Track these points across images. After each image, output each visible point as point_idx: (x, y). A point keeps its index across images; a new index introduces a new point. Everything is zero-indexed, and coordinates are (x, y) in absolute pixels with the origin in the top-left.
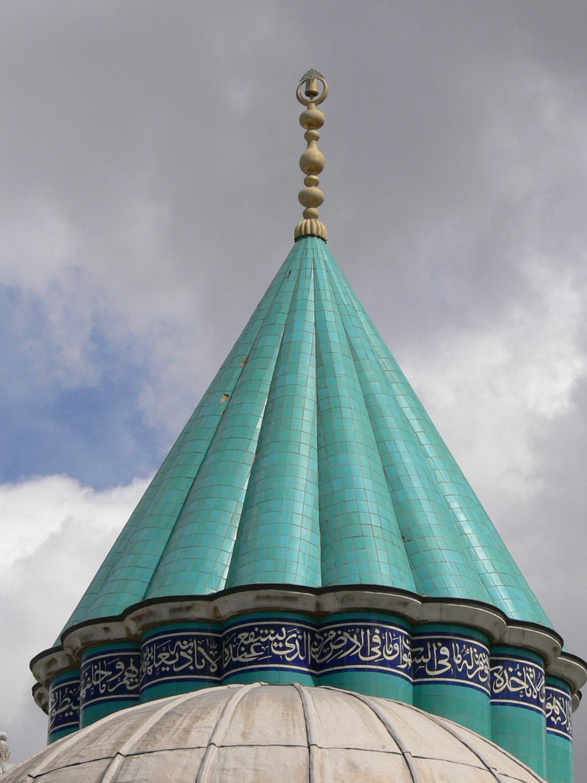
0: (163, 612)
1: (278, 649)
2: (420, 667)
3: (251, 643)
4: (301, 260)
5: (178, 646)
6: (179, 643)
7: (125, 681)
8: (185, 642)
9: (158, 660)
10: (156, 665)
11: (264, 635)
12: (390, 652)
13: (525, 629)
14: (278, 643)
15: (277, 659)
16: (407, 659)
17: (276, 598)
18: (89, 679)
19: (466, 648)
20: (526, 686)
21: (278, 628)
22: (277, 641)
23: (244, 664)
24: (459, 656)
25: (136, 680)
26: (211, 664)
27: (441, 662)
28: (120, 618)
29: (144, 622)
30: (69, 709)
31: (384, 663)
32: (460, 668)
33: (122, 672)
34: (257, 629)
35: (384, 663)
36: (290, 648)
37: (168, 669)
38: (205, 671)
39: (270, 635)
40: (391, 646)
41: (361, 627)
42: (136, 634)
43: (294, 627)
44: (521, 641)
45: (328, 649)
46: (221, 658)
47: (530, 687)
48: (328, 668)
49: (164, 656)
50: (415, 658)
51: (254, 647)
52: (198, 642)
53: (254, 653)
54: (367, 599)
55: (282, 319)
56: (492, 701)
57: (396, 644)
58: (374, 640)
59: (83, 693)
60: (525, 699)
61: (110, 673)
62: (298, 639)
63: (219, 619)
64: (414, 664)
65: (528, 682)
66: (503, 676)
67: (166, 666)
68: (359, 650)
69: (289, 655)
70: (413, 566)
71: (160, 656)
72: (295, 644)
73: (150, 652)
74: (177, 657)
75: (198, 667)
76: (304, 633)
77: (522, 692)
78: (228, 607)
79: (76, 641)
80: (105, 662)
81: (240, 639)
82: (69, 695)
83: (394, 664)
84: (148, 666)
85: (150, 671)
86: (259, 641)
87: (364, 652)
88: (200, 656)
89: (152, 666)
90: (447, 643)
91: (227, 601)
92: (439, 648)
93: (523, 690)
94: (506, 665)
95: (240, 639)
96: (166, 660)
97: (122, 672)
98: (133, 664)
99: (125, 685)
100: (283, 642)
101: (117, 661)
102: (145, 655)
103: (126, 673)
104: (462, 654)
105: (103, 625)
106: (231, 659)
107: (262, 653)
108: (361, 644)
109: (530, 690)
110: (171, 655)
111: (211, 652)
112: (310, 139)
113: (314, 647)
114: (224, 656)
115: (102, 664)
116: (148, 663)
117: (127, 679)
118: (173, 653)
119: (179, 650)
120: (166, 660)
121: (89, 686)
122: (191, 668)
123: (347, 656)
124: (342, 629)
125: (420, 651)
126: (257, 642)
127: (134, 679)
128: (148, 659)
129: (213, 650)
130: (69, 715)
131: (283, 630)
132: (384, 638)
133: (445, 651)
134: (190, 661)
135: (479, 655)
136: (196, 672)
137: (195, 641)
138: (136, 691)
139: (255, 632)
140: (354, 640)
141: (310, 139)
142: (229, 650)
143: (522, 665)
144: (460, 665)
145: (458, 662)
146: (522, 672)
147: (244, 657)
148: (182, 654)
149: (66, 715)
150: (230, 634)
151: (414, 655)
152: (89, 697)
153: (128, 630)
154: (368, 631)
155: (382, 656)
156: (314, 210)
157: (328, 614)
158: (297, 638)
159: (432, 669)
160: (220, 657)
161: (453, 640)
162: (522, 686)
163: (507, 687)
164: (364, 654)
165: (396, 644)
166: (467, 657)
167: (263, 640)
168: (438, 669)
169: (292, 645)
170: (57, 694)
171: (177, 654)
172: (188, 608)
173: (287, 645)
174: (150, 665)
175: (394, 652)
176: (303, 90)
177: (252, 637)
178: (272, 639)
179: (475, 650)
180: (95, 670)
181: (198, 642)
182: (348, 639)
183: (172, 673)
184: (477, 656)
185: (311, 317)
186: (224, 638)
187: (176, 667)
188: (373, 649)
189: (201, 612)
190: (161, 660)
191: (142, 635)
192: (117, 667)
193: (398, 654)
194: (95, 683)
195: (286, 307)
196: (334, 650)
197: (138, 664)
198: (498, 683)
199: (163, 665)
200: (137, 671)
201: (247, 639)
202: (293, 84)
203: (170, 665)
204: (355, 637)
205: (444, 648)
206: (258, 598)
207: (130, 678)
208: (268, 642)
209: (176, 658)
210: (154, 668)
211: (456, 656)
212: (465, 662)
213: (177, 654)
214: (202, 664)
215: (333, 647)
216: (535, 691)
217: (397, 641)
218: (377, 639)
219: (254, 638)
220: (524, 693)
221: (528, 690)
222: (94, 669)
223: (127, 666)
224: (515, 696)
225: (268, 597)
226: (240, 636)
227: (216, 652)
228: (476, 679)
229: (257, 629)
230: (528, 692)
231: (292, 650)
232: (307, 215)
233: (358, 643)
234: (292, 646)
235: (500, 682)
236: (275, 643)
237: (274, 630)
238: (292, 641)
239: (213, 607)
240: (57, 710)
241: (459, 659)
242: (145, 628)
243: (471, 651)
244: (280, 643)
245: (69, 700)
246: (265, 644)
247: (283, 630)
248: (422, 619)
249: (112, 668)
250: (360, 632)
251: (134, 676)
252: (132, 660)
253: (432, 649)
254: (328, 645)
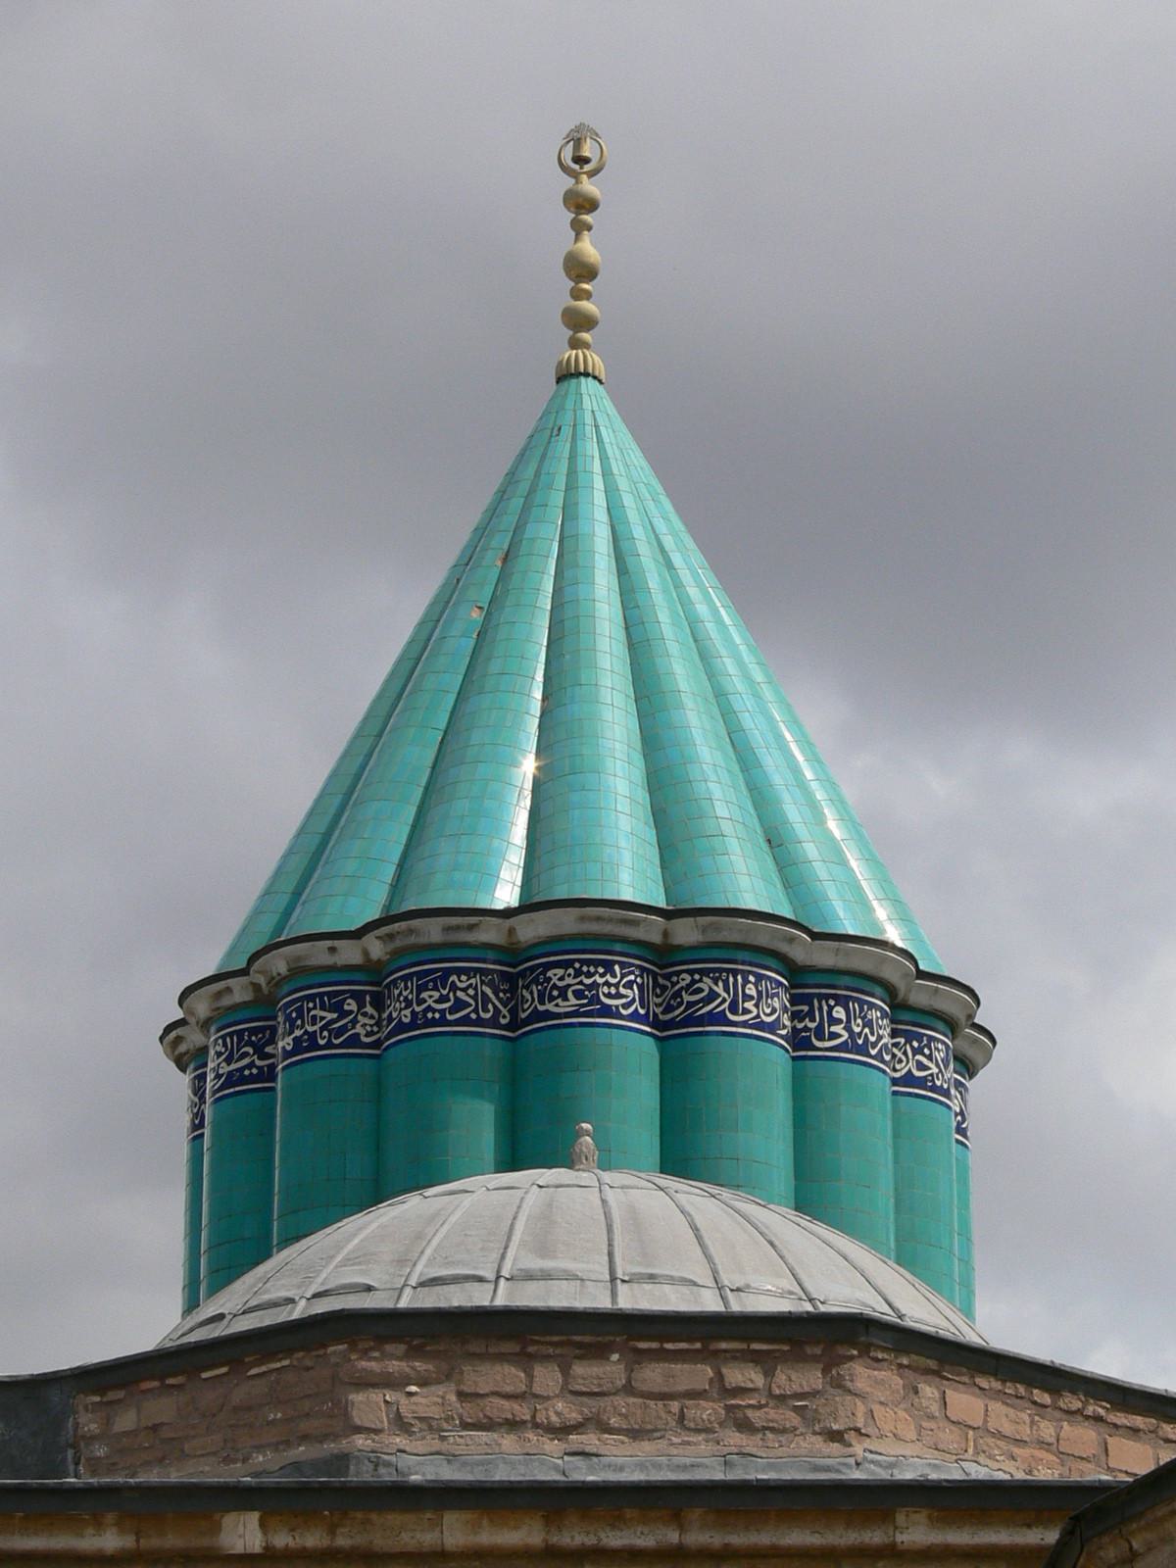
0: (433, 931)
1: (609, 996)
2: (803, 1034)
3: (569, 986)
4: (575, 411)
5: (453, 982)
6: (454, 978)
7: (358, 1029)
8: (463, 978)
9: (420, 1002)
10: (418, 1009)
11: (589, 975)
12: (768, 1011)
13: (940, 986)
14: (609, 988)
15: (607, 1011)
16: (786, 1020)
17: (610, 920)
18: (299, 1022)
19: (868, 1010)
20: (936, 1070)
21: (608, 967)
22: (607, 983)
23: (558, 1016)
24: (859, 1021)
25: (375, 1029)
26: (500, 1011)
27: (834, 1029)
28: (357, 934)
29: (398, 943)
30: (251, 1065)
31: (761, 1026)
32: (860, 1038)
33: (353, 1015)
34: (577, 965)
35: (761, 1026)
36: (623, 996)
37: (437, 1015)
38: (494, 1022)
39: (597, 975)
40: (769, 1001)
41: (728, 971)
42: (379, 960)
43: (633, 965)
44: (932, 1003)
45: (679, 1000)
46: (516, 1004)
47: (940, 1071)
48: (677, 1028)
49: (431, 997)
50: (796, 1021)
51: (573, 991)
52: (483, 978)
53: (573, 1001)
54: (740, 931)
55: (557, 498)
56: (896, 1088)
57: (776, 999)
58: (747, 991)
59: (285, 1043)
60: (934, 1088)
61: (335, 1015)
62: (637, 983)
63: (515, 946)
64: (794, 1028)
65: (938, 1066)
66: (905, 1053)
67: (434, 1011)
68: (726, 1004)
69: (626, 1006)
70: (787, 884)
71: (424, 995)
72: (632, 989)
73: (406, 988)
74: (452, 998)
75: (482, 1015)
76: (645, 975)
77: (930, 1078)
78: (531, 929)
79: (277, 962)
80: (326, 998)
81: (550, 979)
82: (250, 1043)
83: (772, 1028)
84: (401, 1010)
85: (405, 1016)
86: (581, 983)
87: (733, 1008)
88: (486, 999)
89: (410, 1009)
90: (842, 1001)
91: (532, 920)
92: (831, 1008)
93: (932, 1075)
94: (910, 1037)
95: (550, 979)
96: (435, 1002)
97: (353, 1015)
98: (371, 1004)
99: (358, 1035)
100: (617, 986)
101: (345, 999)
102: (397, 992)
103: (360, 1017)
104: (863, 1019)
105: (329, 943)
106: (536, 1006)
107: (586, 1001)
108: (729, 994)
109: (940, 1075)
110: (441, 995)
111: (501, 995)
112: (579, 228)
113: (658, 996)
114: (522, 1001)
115: (322, 1003)
116: (403, 1005)
117: (362, 1026)
118: (445, 992)
119: (454, 988)
120: (435, 1002)
121: (298, 1033)
122: (474, 1016)
123: (708, 1012)
124: (703, 972)
125: (803, 1011)
126: (578, 984)
127: (371, 1026)
128: (402, 999)
129: (505, 993)
130: (251, 1074)
131: (617, 967)
132: (760, 989)
133: (839, 1013)
134: (471, 1005)
135: (882, 1020)
136: (480, 1022)
137: (478, 977)
138: (376, 1044)
139: (574, 968)
140: (719, 989)
141: (579, 228)
142: (532, 993)
143: (931, 1039)
144: (860, 1034)
145: (857, 1030)
146: (930, 1049)
147: (557, 1005)
148: (459, 994)
149: (247, 1072)
150: (532, 969)
151: (796, 1016)
152: (297, 1048)
153: (366, 953)
154: (739, 977)
155: (758, 1016)
156: (586, 336)
157: (679, 948)
158: (635, 981)
159: (821, 1038)
160: (513, 1002)
161: (851, 997)
162: (930, 1069)
163: (910, 1070)
164: (734, 1011)
165: (776, 999)
166: (868, 1024)
167: (588, 981)
168: (830, 1039)
169: (629, 991)
170: (228, 1040)
171: (451, 994)
172: (471, 927)
173: (622, 990)
174: (406, 1008)
175: (774, 1011)
176: (568, 155)
177: (569, 975)
178: (601, 981)
179: (879, 1014)
180: (309, 1010)
181: (483, 978)
182: (710, 988)
183: (443, 1022)
184: (880, 1021)
185: (600, 499)
186: (522, 974)
187: (450, 1014)
188: (746, 1005)
189: (490, 933)
190: (426, 1001)
191: (389, 961)
192: (346, 1007)
193: (777, 1014)
194: (310, 1029)
195: (561, 482)
196: (688, 1002)
197: (379, 1003)
198: (898, 1063)
199: (429, 1009)
200: (376, 1015)
201: (561, 979)
202: (552, 144)
203: (442, 1010)
204: (720, 984)
205: (838, 1008)
206: (583, 919)
207: (366, 1024)
208: (595, 985)
209: (449, 1000)
210: (413, 1013)
211: (855, 1020)
212: (867, 1030)
213: (451, 994)
214: (489, 1011)
215: (687, 998)
216: (945, 1077)
217: (777, 995)
218: (751, 990)
219: (574, 978)
220: (933, 1080)
221: (937, 1075)
222: (308, 1008)
223: (361, 1005)
224: (921, 1083)
225: (598, 919)
226: (550, 974)
227: (508, 995)
228: (879, 1057)
229: (577, 965)
230: (938, 1079)
231: (629, 999)
232: (575, 344)
233: (726, 996)
234: (628, 992)
235: (900, 1061)
236: (605, 987)
237: (603, 967)
238: (629, 985)
239: (507, 928)
240: (229, 1065)
241: (858, 1025)
242: (396, 953)
243: (875, 1014)
244: (612, 988)
245: (250, 1050)
246: (590, 987)
247: (617, 967)
248: (808, 964)
249: (338, 1008)
250: (728, 978)
251: (372, 1022)
252: (368, 998)
253: (821, 1009)
254: (678, 994)
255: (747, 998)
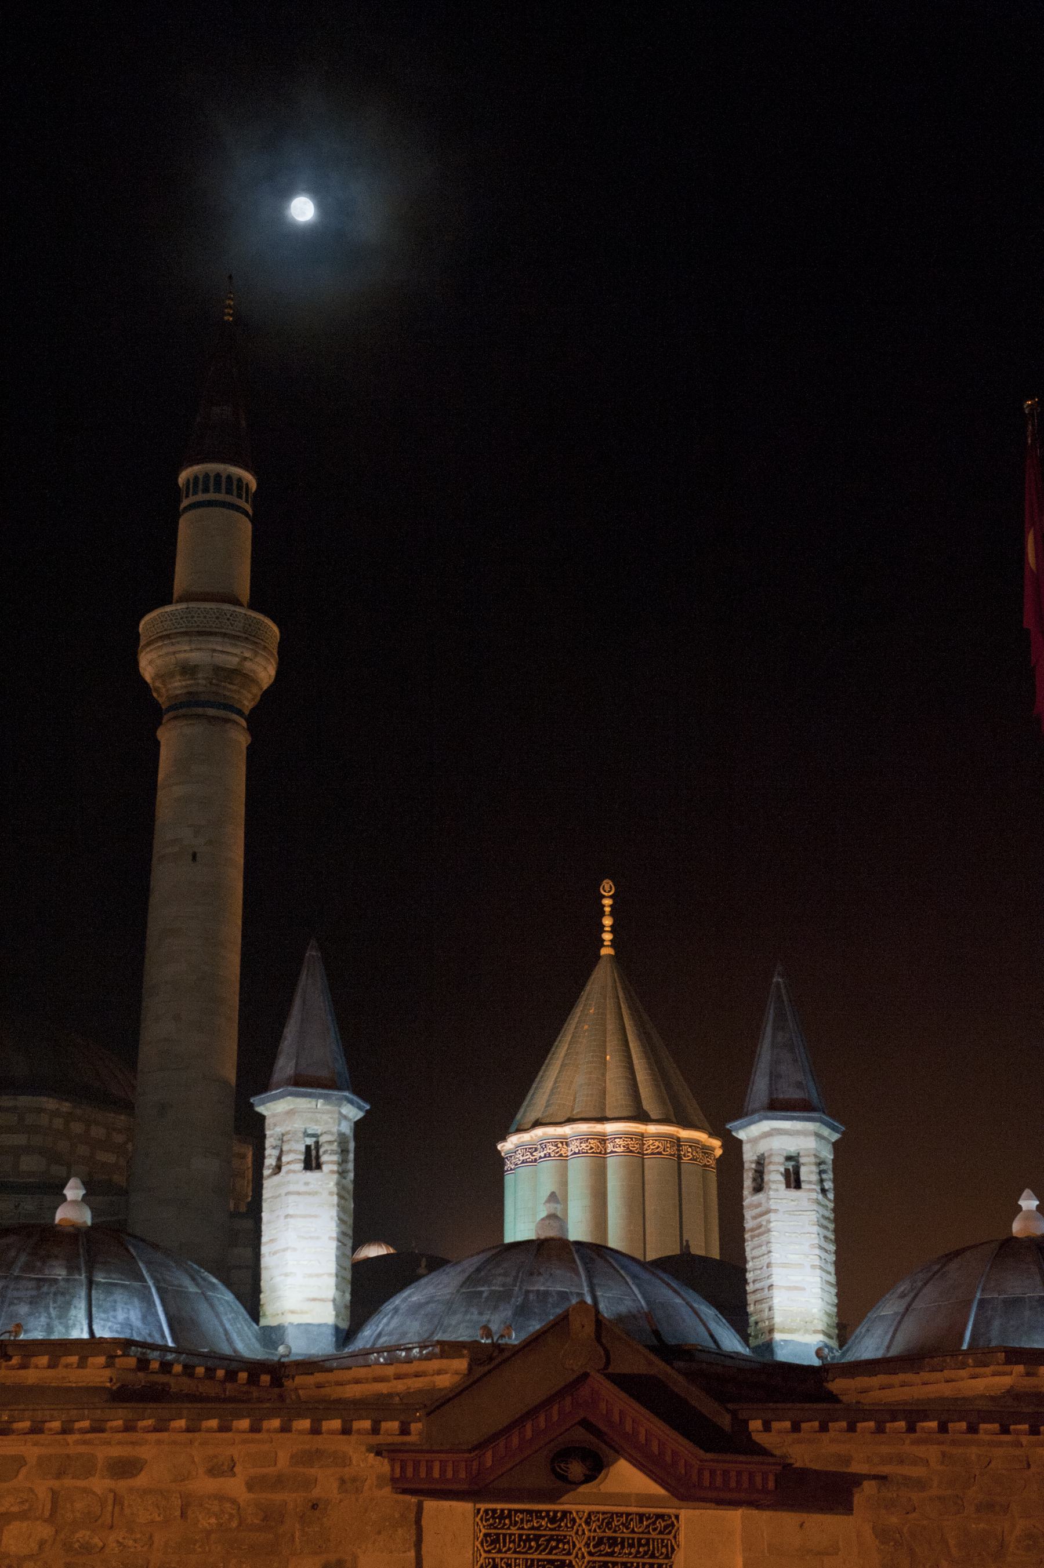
30: (529, 1158)
53: (622, 1148)
88: (598, 1147)
119: (590, 1143)
183: (587, 1153)
215: (652, 1147)
249: (556, 1146)
255: (668, 1147)
